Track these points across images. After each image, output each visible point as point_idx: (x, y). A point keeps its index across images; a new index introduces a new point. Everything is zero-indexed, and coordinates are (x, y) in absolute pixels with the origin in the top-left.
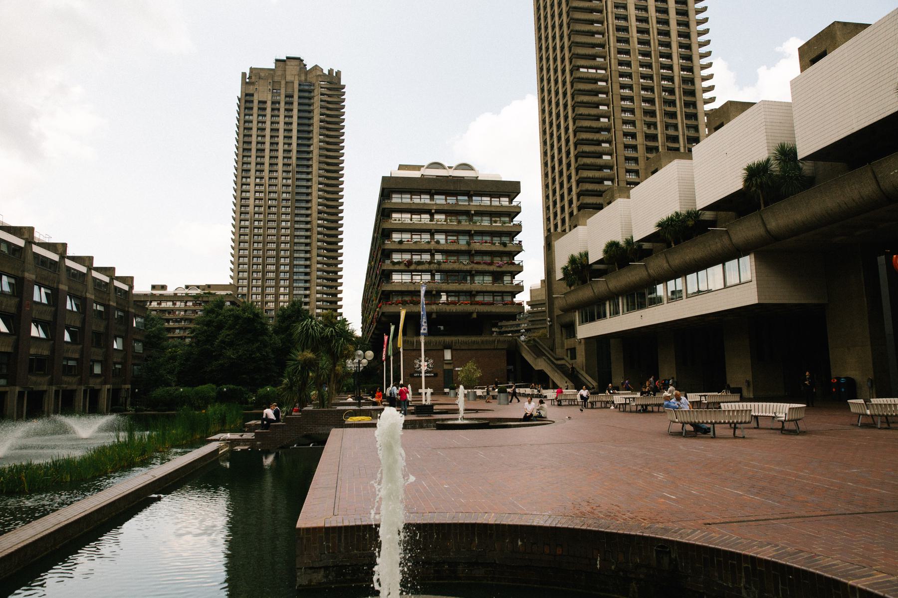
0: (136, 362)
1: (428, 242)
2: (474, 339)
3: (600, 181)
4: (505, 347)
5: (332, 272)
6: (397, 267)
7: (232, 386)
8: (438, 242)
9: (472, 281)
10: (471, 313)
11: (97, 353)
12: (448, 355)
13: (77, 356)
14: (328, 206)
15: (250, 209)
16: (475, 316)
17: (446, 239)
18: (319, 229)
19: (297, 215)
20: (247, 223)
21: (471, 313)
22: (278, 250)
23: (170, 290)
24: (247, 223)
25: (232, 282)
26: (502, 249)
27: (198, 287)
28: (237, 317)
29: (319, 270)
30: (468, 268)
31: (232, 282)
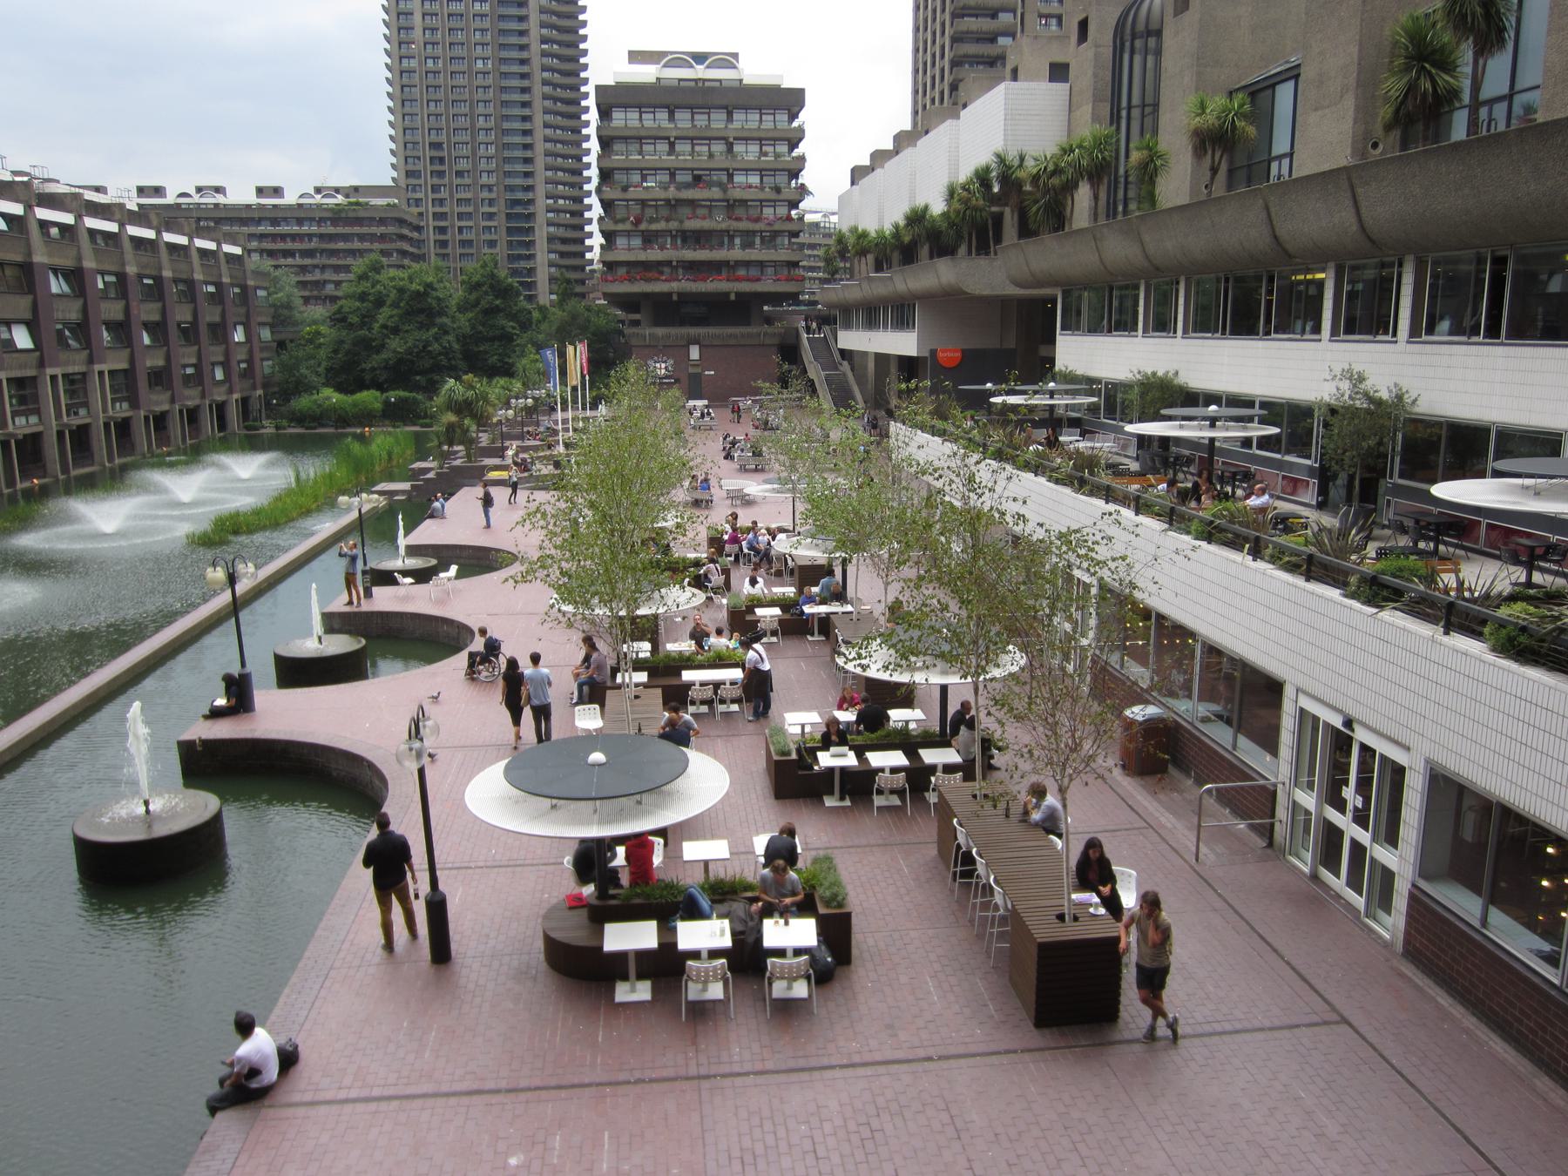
0: (265, 355)
3: (992, 39)
4: (776, 341)
5: (572, 157)
6: (620, 227)
7: (402, 393)
9: (731, 246)
10: (727, 294)
11: (215, 353)
12: (695, 353)
13: (193, 361)
14: (559, 29)
15: (417, 33)
16: (733, 297)
18: (546, 75)
22: (472, 116)
23: (290, 198)
25: (395, 174)
26: (773, 196)
27: (337, 190)
28: (401, 291)
30: (723, 226)
31: (395, 174)
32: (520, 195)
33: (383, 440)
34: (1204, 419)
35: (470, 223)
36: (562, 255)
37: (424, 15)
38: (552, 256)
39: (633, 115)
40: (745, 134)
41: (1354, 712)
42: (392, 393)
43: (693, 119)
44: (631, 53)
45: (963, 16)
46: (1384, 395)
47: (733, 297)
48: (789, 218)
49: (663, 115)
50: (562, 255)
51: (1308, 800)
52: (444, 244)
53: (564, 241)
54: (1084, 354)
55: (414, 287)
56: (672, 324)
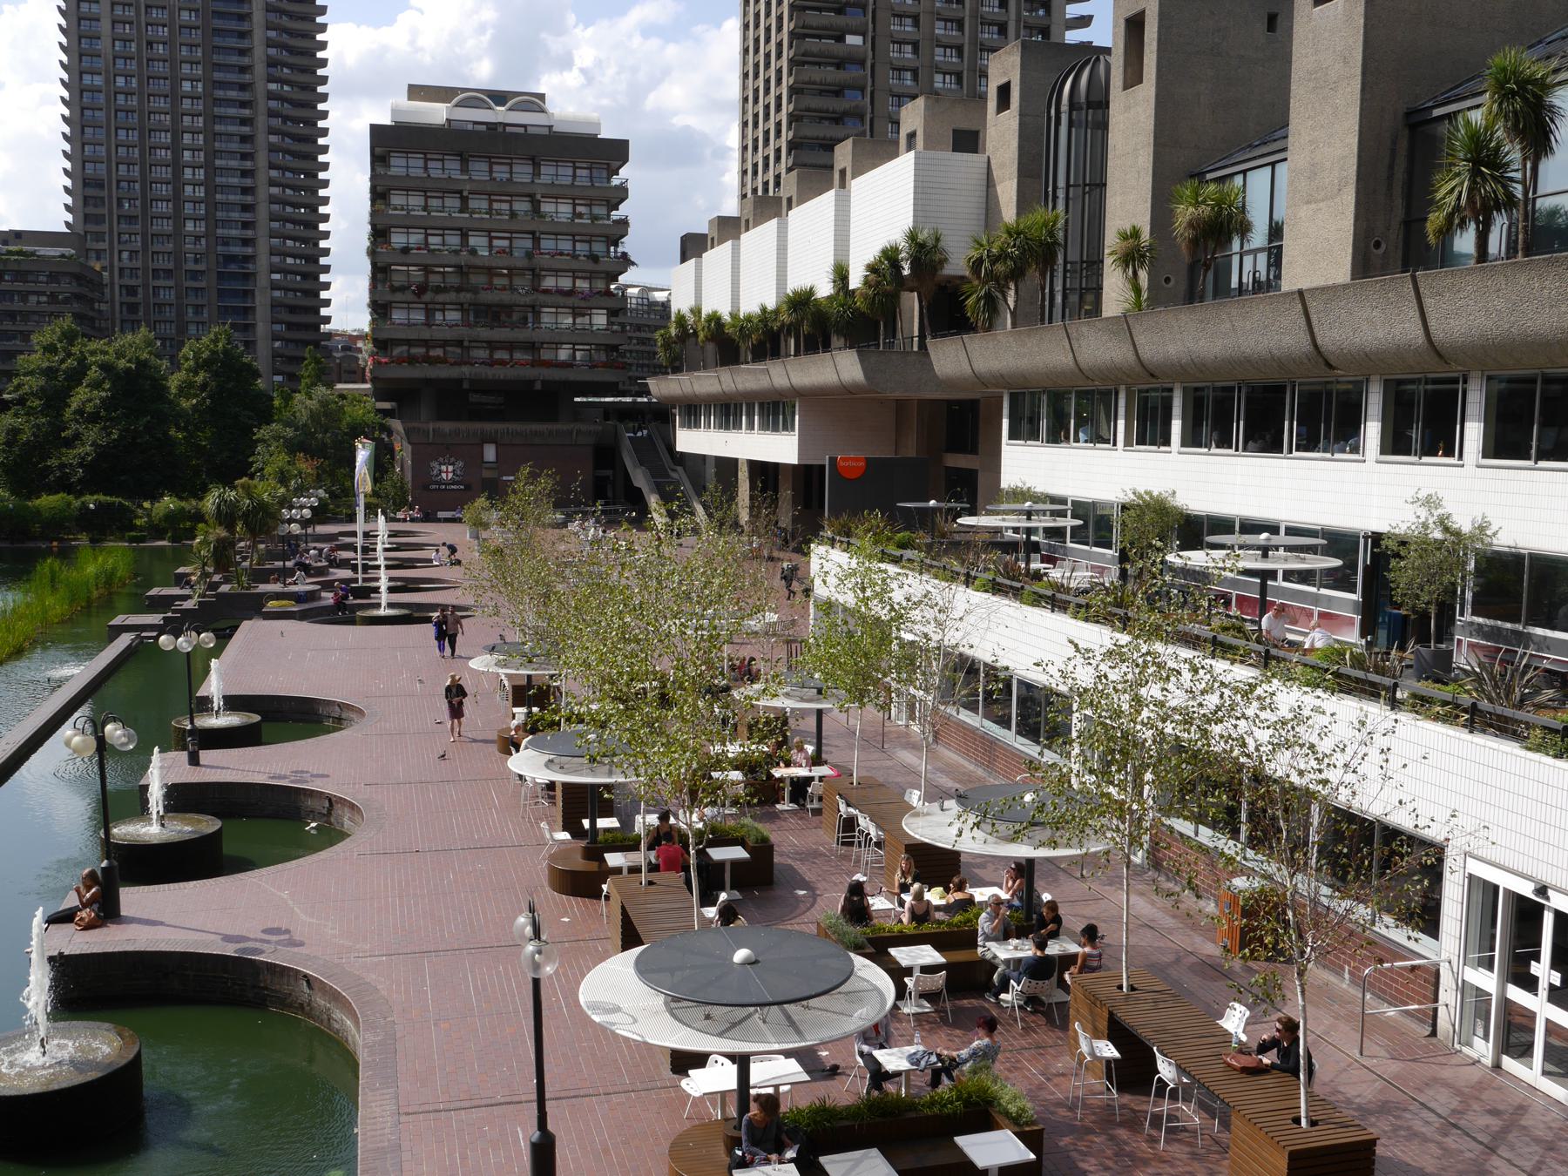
1: (456, 252)
2: (536, 427)
6: (399, 296)
7: (102, 498)
8: (473, 252)
12: (490, 453)
15: (104, 45)
16: (538, 386)
17: (491, 246)
19: (219, 67)
20: (98, 81)
21: (531, 382)
24: (98, 81)
26: (590, 266)
29: (273, 200)
31: (69, 218)
32: (236, 250)
33: (98, 562)
34: (1259, 548)
35: (171, 283)
36: (290, 326)
37: (114, 22)
38: (277, 327)
39: (416, 163)
40: (554, 191)
41: (1547, 877)
42: (87, 498)
43: (491, 171)
44: (411, 87)
45: (804, 63)
46: (1466, 528)
47: (538, 386)
48: (608, 293)
49: (453, 166)
50: (290, 326)
51: (1487, 981)
52: (133, 308)
53: (292, 309)
54: (1029, 466)
55: (122, 364)
56: (458, 418)
